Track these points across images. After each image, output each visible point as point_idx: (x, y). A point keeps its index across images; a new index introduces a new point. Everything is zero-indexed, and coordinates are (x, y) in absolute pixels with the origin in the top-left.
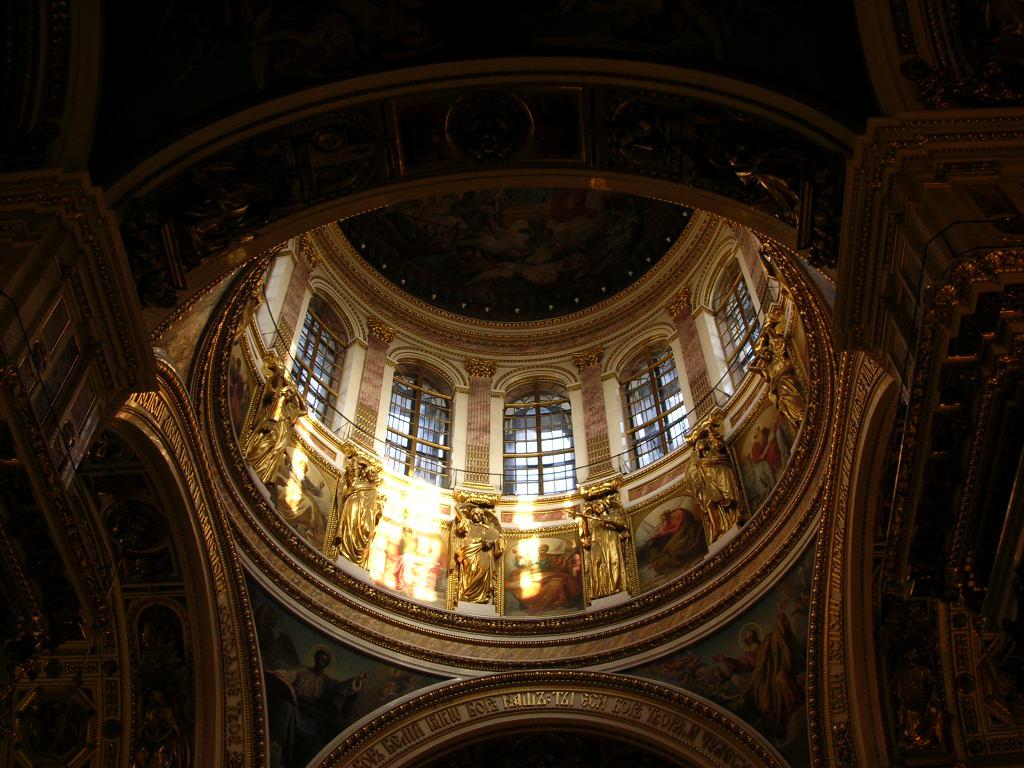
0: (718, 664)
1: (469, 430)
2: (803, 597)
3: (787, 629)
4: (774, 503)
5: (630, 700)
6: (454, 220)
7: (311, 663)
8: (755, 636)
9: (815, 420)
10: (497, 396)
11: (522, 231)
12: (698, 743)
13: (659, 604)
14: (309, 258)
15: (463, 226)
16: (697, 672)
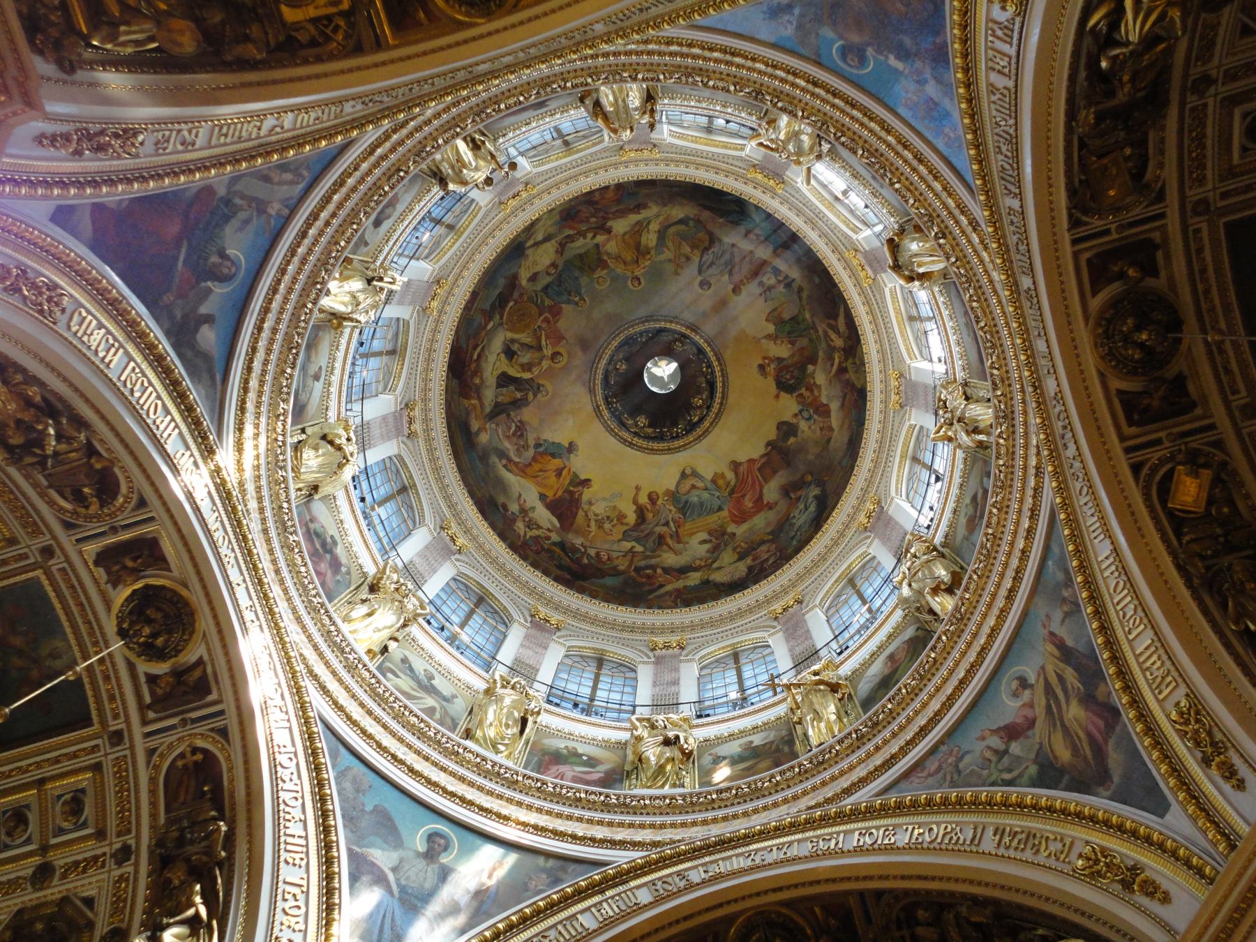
0: (985, 743)
1: (655, 684)
2: (1066, 594)
3: (1061, 645)
4: (994, 520)
5: (878, 828)
6: (627, 545)
7: (421, 847)
8: (1023, 683)
9: (1002, 381)
10: (689, 661)
11: (704, 542)
12: (989, 843)
13: (892, 715)
14: (453, 540)
15: (639, 548)
16: (961, 765)
